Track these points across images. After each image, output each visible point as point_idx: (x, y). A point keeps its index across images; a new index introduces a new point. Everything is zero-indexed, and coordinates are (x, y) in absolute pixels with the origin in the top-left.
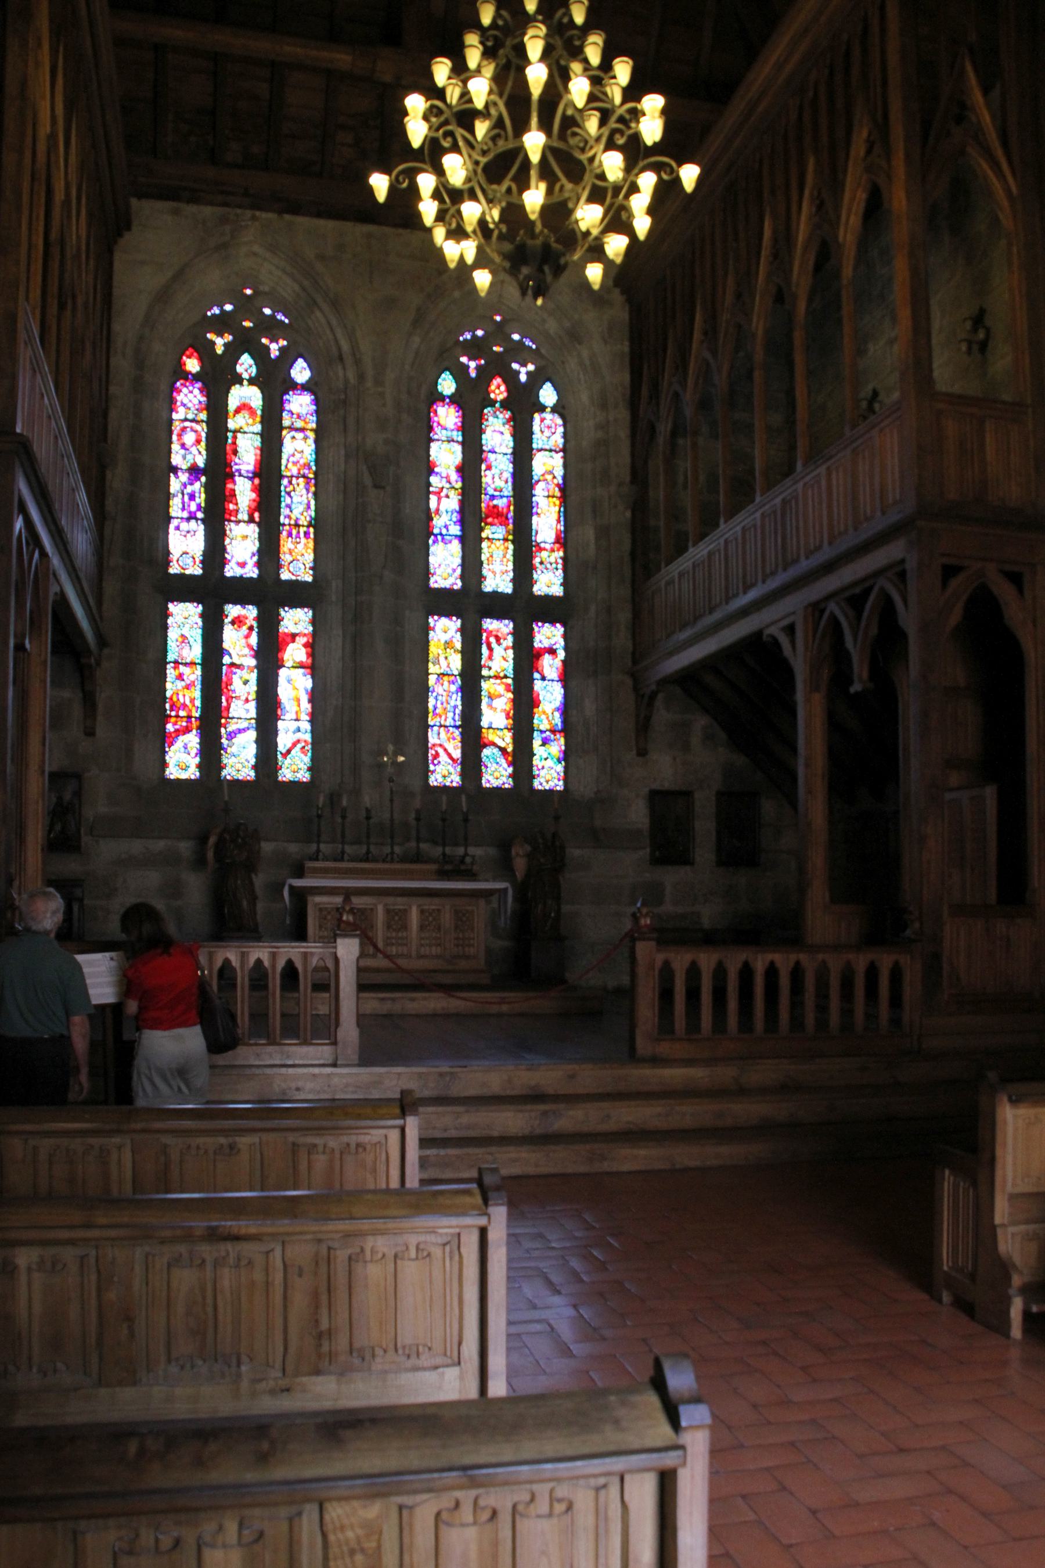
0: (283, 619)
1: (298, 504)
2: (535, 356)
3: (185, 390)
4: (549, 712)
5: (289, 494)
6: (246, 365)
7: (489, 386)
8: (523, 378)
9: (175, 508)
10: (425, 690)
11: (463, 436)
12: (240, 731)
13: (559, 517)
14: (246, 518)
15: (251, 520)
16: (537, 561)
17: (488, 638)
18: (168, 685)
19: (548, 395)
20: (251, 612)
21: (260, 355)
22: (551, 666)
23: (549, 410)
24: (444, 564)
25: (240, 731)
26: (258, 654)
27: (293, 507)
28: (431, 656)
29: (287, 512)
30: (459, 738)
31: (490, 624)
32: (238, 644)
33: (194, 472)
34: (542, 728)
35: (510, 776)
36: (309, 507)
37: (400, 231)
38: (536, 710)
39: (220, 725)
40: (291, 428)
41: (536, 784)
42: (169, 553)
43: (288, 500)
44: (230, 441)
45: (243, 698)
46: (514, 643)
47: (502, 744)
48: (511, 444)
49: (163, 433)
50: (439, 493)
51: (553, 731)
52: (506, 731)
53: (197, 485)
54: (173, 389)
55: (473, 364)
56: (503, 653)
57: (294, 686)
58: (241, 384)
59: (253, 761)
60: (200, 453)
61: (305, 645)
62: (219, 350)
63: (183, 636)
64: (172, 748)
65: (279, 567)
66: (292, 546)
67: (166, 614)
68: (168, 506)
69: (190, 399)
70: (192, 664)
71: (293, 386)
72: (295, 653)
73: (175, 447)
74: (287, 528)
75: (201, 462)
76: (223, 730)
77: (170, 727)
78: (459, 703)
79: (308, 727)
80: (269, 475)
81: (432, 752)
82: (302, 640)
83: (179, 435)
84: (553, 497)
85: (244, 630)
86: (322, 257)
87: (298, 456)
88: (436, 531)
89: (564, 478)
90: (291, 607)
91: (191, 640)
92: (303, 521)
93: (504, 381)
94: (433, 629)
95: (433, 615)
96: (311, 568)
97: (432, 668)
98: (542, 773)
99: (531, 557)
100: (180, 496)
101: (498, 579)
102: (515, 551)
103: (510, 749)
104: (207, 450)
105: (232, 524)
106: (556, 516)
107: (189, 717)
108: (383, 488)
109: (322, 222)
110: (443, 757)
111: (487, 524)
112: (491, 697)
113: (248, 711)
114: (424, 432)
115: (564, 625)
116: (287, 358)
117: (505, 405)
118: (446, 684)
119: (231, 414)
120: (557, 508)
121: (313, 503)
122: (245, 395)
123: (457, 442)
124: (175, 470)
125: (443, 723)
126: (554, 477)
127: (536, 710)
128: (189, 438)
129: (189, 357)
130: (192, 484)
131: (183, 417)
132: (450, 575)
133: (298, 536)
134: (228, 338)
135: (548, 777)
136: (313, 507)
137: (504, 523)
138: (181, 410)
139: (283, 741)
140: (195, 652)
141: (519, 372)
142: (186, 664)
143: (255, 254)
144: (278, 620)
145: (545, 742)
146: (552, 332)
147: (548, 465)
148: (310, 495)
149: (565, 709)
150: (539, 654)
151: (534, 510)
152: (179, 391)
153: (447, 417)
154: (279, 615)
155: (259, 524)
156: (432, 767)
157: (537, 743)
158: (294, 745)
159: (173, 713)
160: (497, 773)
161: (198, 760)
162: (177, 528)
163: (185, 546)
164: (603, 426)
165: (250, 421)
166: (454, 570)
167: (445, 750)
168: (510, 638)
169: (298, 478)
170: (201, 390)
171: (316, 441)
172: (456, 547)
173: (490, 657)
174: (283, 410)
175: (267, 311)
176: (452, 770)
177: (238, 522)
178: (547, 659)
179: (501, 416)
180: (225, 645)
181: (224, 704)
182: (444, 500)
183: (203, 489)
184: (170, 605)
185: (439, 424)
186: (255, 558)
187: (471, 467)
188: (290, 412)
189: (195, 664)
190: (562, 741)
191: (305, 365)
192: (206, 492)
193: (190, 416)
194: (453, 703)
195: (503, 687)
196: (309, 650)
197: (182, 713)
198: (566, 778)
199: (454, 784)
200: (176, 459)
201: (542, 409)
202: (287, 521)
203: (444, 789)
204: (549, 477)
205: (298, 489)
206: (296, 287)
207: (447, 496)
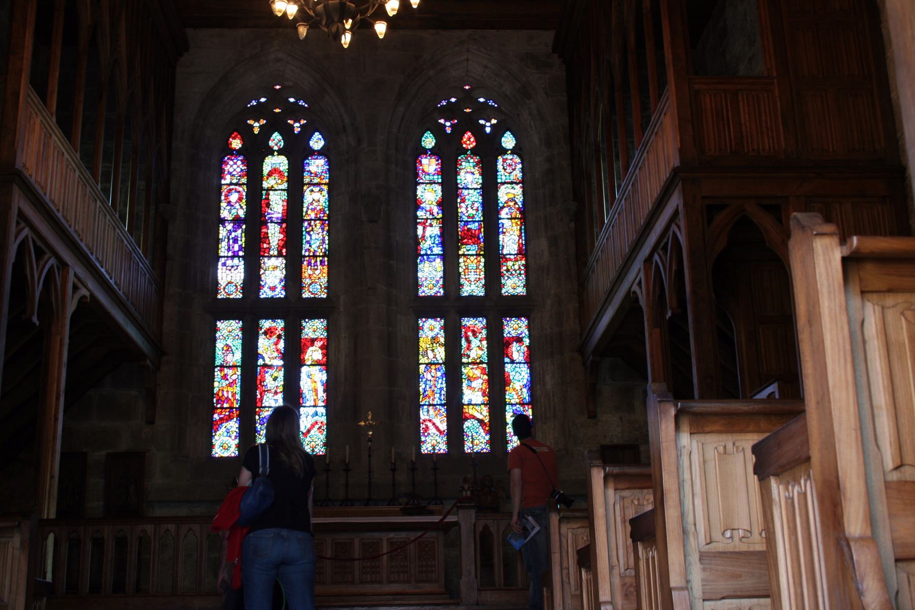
1: (316, 240)
3: (231, 163)
4: (518, 388)
5: (308, 233)
6: (276, 140)
7: (462, 139)
8: (488, 130)
9: (223, 251)
10: (417, 377)
11: (442, 178)
14: (276, 253)
15: (280, 255)
17: (466, 333)
18: (216, 384)
19: (508, 141)
20: (280, 324)
21: (287, 132)
22: (518, 352)
24: (430, 276)
26: (284, 356)
27: (312, 242)
28: (421, 349)
29: (307, 246)
30: (445, 414)
31: (468, 322)
32: (269, 349)
33: (237, 221)
34: (513, 402)
36: (324, 242)
39: (256, 413)
40: (310, 184)
42: (217, 283)
43: (308, 238)
46: (487, 334)
47: (481, 417)
49: (213, 195)
50: (424, 223)
52: (483, 406)
53: (240, 231)
54: (222, 162)
55: (448, 124)
56: (479, 343)
58: (273, 155)
60: (241, 207)
61: (321, 348)
62: (256, 131)
63: (227, 345)
64: (218, 433)
65: (301, 288)
66: (310, 272)
67: (215, 329)
68: (218, 249)
71: (312, 153)
72: (314, 354)
73: (223, 204)
75: (242, 214)
76: (257, 417)
77: (216, 416)
78: (444, 385)
79: (323, 410)
80: (293, 220)
81: (423, 426)
82: (319, 344)
83: (227, 196)
84: (515, 218)
85: (274, 339)
87: (315, 204)
88: (423, 252)
89: (524, 203)
90: (310, 319)
91: (234, 348)
93: (473, 134)
94: (422, 328)
95: (421, 318)
97: (422, 360)
99: (500, 266)
101: (473, 285)
105: (266, 259)
106: (518, 233)
110: (432, 430)
111: (463, 244)
112: (470, 379)
113: (276, 400)
115: (527, 318)
116: (307, 133)
117: (474, 152)
118: (433, 371)
121: (327, 238)
122: (277, 162)
123: (438, 183)
124: (223, 221)
126: (516, 203)
127: (507, 388)
128: (234, 197)
129: (234, 138)
130: (235, 231)
132: (434, 286)
133: (315, 264)
134: (263, 122)
136: (327, 242)
137: (476, 242)
138: (228, 177)
140: (236, 357)
141: (485, 126)
142: (229, 367)
144: (300, 329)
147: (510, 194)
150: (508, 343)
153: (430, 165)
155: (285, 257)
156: (423, 439)
158: (313, 426)
159: (219, 406)
160: (477, 440)
161: (237, 441)
162: (224, 264)
163: (230, 277)
167: (434, 424)
168: (484, 332)
169: (315, 220)
171: (329, 193)
172: (438, 264)
173: (469, 348)
174: (303, 170)
177: (270, 257)
178: (515, 346)
180: (260, 351)
181: (259, 396)
182: (428, 229)
185: (423, 171)
186: (283, 284)
188: (309, 171)
189: (236, 366)
191: (320, 137)
193: (234, 181)
194: (439, 386)
196: (325, 351)
197: (225, 405)
199: (442, 451)
200: (224, 214)
202: (307, 254)
203: (433, 457)
204: (512, 204)
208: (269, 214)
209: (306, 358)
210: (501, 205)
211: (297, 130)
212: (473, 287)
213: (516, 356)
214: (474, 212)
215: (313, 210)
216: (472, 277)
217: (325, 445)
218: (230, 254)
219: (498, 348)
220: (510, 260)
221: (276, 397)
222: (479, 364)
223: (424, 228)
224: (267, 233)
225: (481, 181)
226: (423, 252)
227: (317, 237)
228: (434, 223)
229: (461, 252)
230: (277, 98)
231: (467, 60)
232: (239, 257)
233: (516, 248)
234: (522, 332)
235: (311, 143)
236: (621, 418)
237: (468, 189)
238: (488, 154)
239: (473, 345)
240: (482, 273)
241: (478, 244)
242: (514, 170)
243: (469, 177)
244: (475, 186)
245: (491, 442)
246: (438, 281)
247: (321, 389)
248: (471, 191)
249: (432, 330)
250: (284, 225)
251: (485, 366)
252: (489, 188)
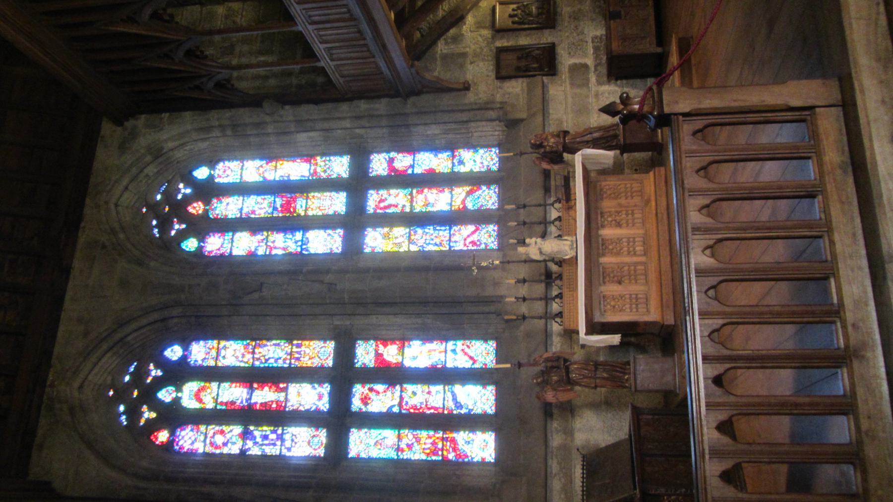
0: (364, 364)
1: (274, 353)
2: (172, 183)
5: (267, 360)
6: (166, 395)
7: (193, 214)
8: (188, 191)
12: (454, 399)
14: (283, 394)
15: (285, 390)
16: (324, 176)
17: (381, 209)
19: (202, 173)
20: (359, 390)
21: (160, 383)
23: (212, 172)
24: (324, 243)
25: (454, 399)
27: (277, 357)
29: (280, 361)
32: (382, 399)
33: (246, 435)
34: (450, 166)
35: (489, 188)
37: (71, 276)
38: (437, 171)
40: (217, 359)
41: (495, 168)
43: (272, 361)
44: (224, 407)
45: (427, 396)
47: (464, 194)
48: (236, 197)
50: (271, 249)
51: (454, 157)
53: (257, 434)
55: (177, 227)
56: (392, 197)
57: (419, 354)
58: (180, 398)
59: (479, 388)
60: (231, 431)
61: (385, 346)
62: (153, 415)
63: (376, 444)
64: (469, 454)
67: (358, 459)
69: (191, 440)
70: (399, 437)
71: (184, 358)
72: (391, 353)
73: (225, 450)
74: (293, 361)
76: (455, 412)
77: (451, 456)
79: (450, 345)
80: (252, 377)
81: (471, 247)
83: (217, 447)
84: (276, 167)
85: (372, 395)
86: (86, 334)
88: (299, 249)
89: (262, 159)
91: (379, 437)
92: (288, 349)
93: (190, 204)
96: (325, 342)
97: (404, 248)
98: (486, 163)
100: (264, 447)
103: (468, 188)
104: (228, 424)
105: (289, 404)
107: (443, 439)
108: (262, 284)
109: (60, 334)
110: (475, 237)
111: (295, 211)
112: (427, 205)
114: (224, 260)
115: (371, 153)
116: (162, 363)
117: (207, 202)
118: (416, 237)
119: (202, 406)
121: (274, 342)
122: (188, 396)
124: (243, 452)
125: (447, 238)
126: (262, 166)
127: (437, 171)
128: (219, 440)
129: (157, 439)
130: (255, 438)
131: (203, 444)
135: (489, 159)
136: (278, 342)
137: (294, 200)
138: (195, 446)
139: (463, 363)
140: (389, 435)
143: (81, 387)
145: (461, 162)
146: (155, 170)
148: (268, 344)
149: (435, 149)
152: (182, 448)
153: (214, 244)
154: (361, 368)
156: (483, 246)
157: (463, 169)
158: (466, 354)
159: (440, 453)
160: (488, 198)
161: (479, 433)
162: (289, 449)
163: (304, 444)
164: (222, 127)
165: (209, 391)
166: (329, 235)
167: (468, 236)
168: (381, 192)
170: (182, 430)
172: (312, 234)
174: (201, 367)
175: (127, 378)
176: (484, 231)
177: (286, 398)
180: (385, 410)
181: (432, 411)
182: (277, 244)
183: (260, 429)
184: (350, 456)
185: (219, 249)
186: (316, 386)
187: (253, 225)
188: (203, 360)
190: (461, 151)
191: (169, 350)
192: (262, 426)
193: (202, 438)
195: (420, 196)
197: (440, 446)
198: (488, 146)
199: (496, 228)
200: (235, 450)
201: (211, 177)
202: (288, 362)
205: (264, 353)
206: (108, 355)
207: (273, 242)
208: (242, 402)
209: (394, 361)
211: (160, 373)
212: (337, 202)
215: (243, 355)
216: (328, 203)
217: (486, 341)
218: (279, 443)
220: (315, 169)
221: (433, 393)
223: (275, 248)
224: (262, 404)
227: (271, 352)
228: (271, 238)
230: (123, 394)
231: (116, 205)
232: (283, 434)
235: (175, 358)
236: (471, 63)
238: (209, 191)
239: (393, 202)
241: (296, 198)
243: (229, 207)
246: (329, 235)
247: (429, 346)
250: (255, 385)
252: (242, 189)
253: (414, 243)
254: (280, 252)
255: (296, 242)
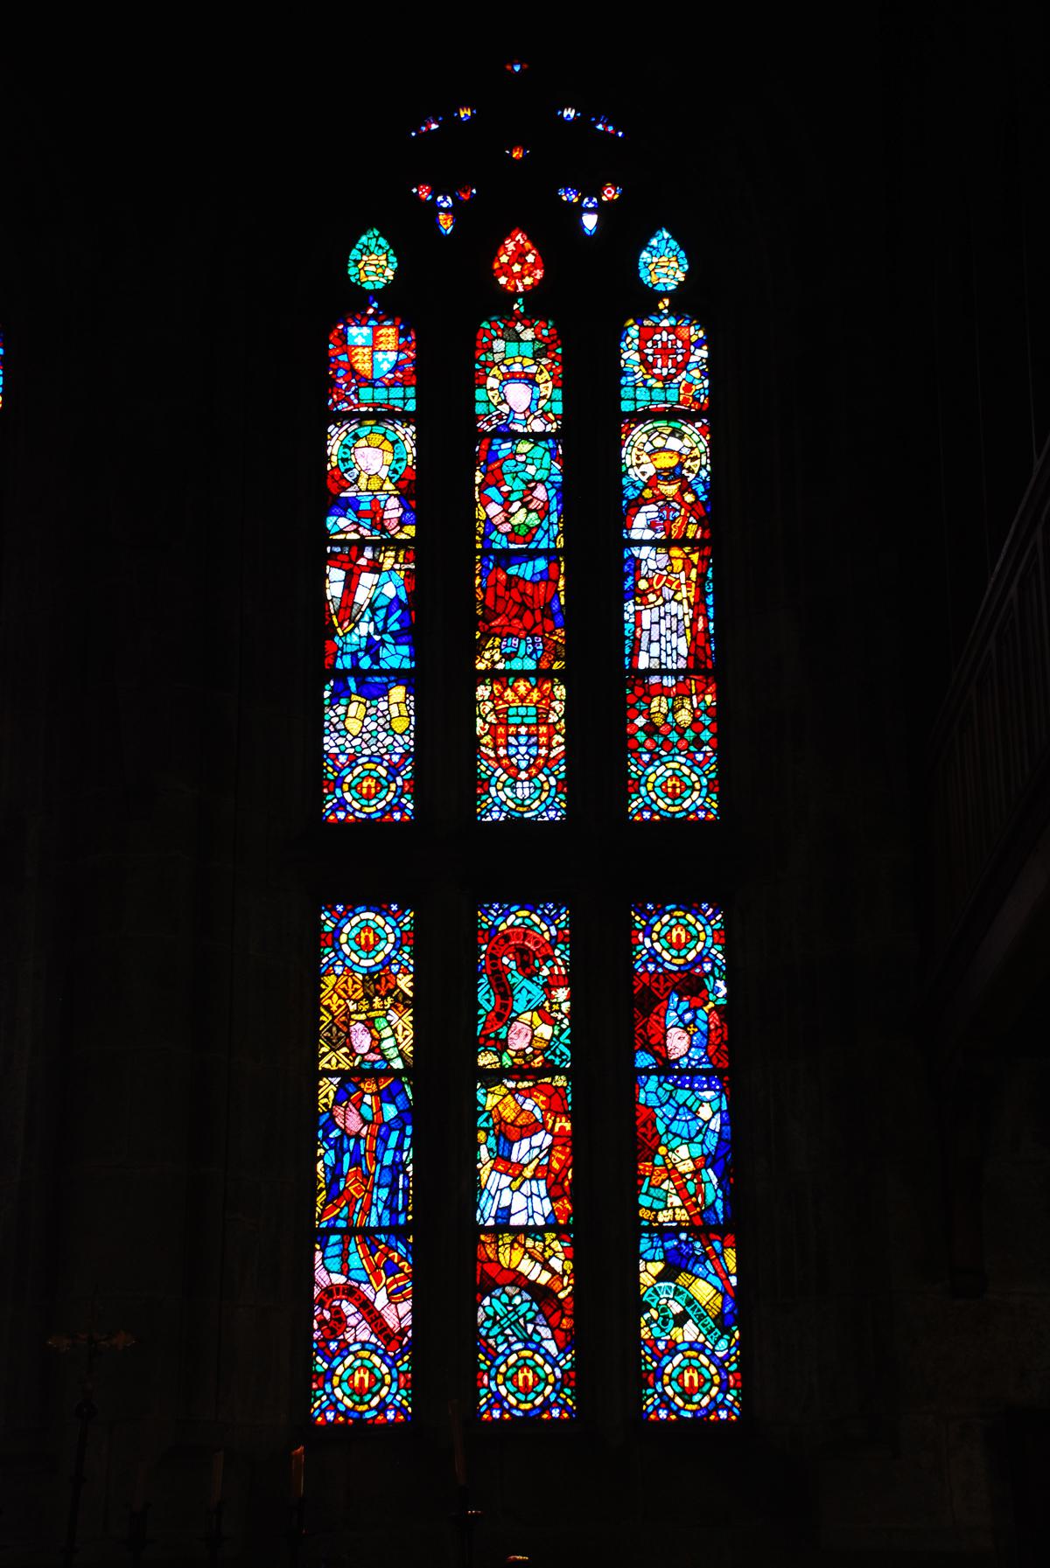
4: (686, 1167)
7: (495, 257)
8: (590, 221)
10: (307, 1125)
11: (419, 397)
13: (702, 594)
17: (494, 958)
19: (663, 264)
28: (326, 1018)
46: (574, 964)
47: (545, 1278)
55: (447, 203)
56: (538, 994)
84: (682, 542)
89: (713, 486)
98: (672, 1366)
99: (619, 716)
101: (521, 786)
102: (569, 702)
111: (487, 636)
114: (309, 398)
117: (539, 304)
120: (693, 574)
123: (405, 417)
126: (686, 487)
141: (580, 210)
145: (675, 1266)
151: (629, 582)
153: (375, 350)
156: (321, 1365)
160: (525, 1371)
166: (394, 770)
167: (366, 1307)
173: (504, 1014)
178: (675, 1009)
179: (528, 334)
182: (367, 579)
185: (352, 371)
203: (355, 1432)
204: (671, 490)
210: (630, 493)
213: (677, 1043)
214: (533, 519)
219: (612, 1011)
220: (663, 691)
222: (537, 1074)
225: (558, 408)
226: (345, 663)
229: (481, 666)
233: (684, 651)
234: (700, 959)
237: (515, 437)
240: (558, 738)
242: (682, 367)
243: (519, 395)
244: (538, 426)
245: (579, 1378)
246: (394, 770)
248: (524, 447)
249: (368, 948)
251: (560, 1081)
253: (341, 1096)
254: (334, 589)
255: (372, 648)
